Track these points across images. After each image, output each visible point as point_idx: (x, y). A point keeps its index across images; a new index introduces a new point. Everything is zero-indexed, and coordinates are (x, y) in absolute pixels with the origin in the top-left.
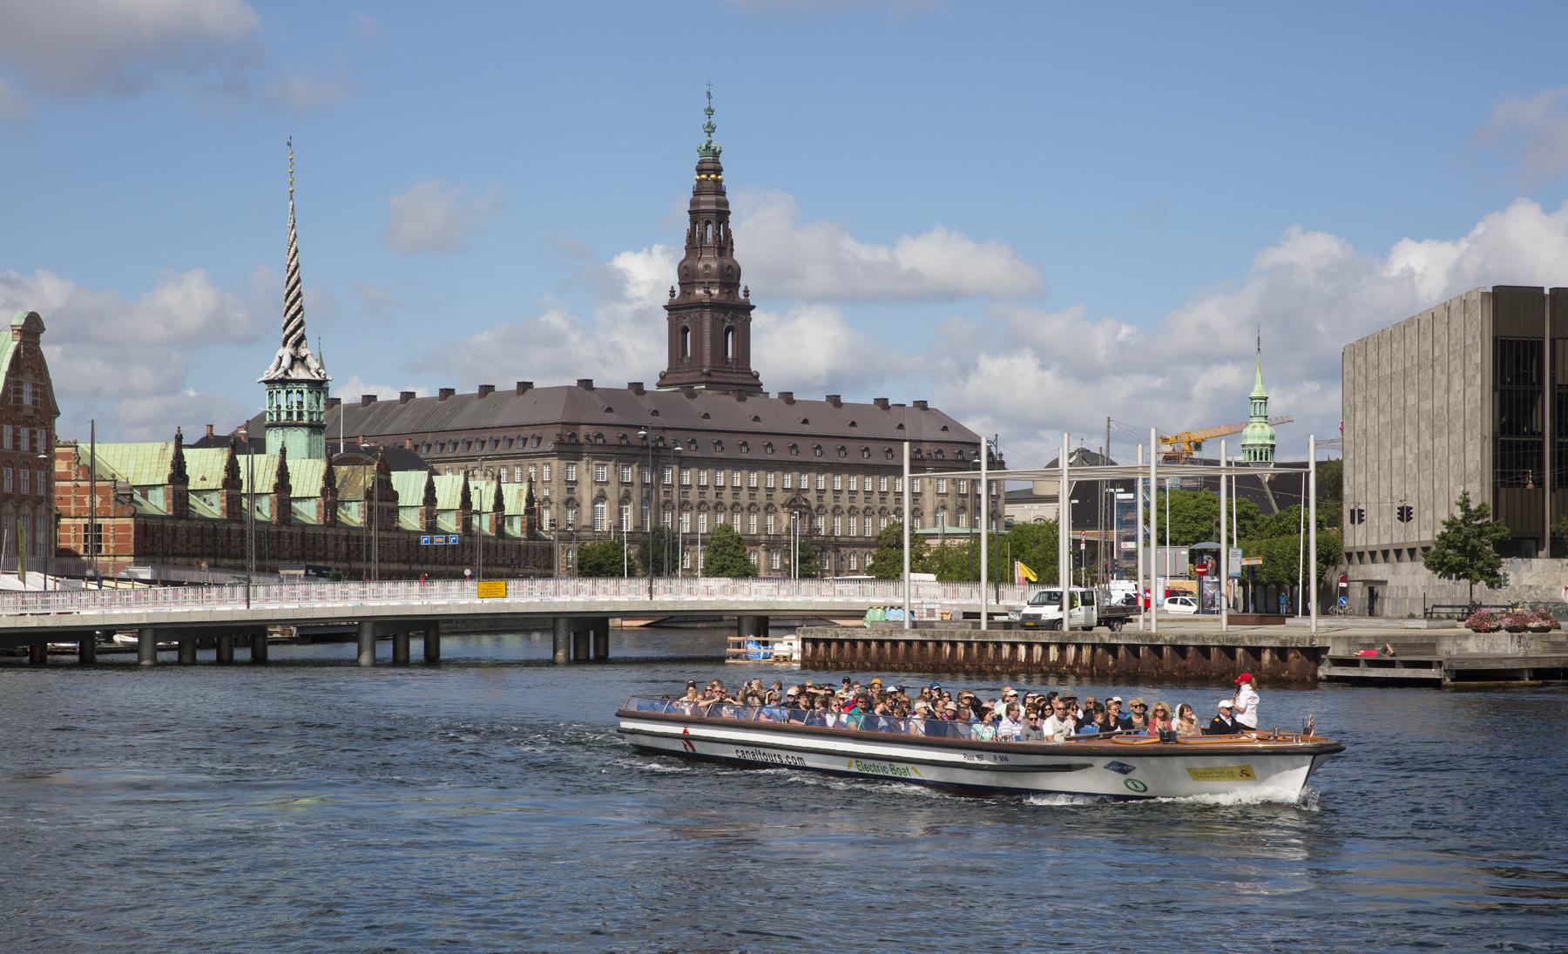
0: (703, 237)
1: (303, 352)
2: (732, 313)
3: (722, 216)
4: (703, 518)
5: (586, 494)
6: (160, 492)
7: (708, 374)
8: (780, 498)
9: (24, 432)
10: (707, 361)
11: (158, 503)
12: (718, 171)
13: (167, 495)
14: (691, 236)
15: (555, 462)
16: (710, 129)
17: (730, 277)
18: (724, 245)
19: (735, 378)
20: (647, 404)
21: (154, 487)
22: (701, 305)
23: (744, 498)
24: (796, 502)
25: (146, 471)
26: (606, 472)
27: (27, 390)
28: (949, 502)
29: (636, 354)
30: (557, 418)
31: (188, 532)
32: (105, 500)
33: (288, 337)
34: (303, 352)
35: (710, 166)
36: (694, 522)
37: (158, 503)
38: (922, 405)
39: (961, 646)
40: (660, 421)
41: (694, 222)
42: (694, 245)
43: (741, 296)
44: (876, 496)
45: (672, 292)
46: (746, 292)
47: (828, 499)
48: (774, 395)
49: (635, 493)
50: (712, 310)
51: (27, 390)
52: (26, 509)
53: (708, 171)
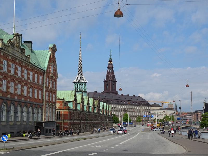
0: (109, 71)
7: (111, 91)
8: (123, 109)
10: (111, 89)
12: (112, 62)
13: (73, 104)
18: (113, 72)
19: (114, 92)
21: (70, 102)
23: (118, 110)
25: (67, 98)
32: (61, 105)
33: (79, 73)
35: (110, 61)
40: (107, 98)
43: (115, 80)
45: (105, 79)
46: (116, 79)
47: (129, 109)
53: (111, 62)
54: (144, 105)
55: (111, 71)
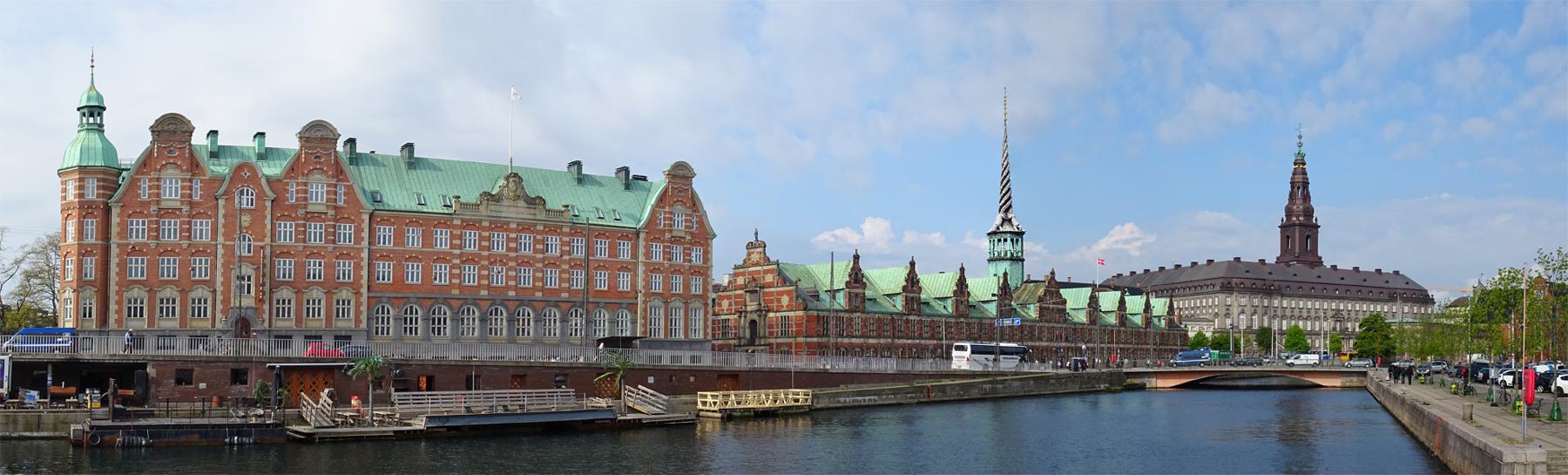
3: (1306, 184)
5: (1235, 310)
8: (1330, 314)
16: (1300, 145)
17: (1309, 212)
18: (1307, 197)
19: (1310, 259)
24: (1337, 316)
26: (1243, 301)
29: (1265, 246)
31: (865, 321)
38: (1397, 273)
40: (1273, 277)
42: (1292, 196)
47: (1353, 315)
49: (1259, 310)
50: (1300, 228)
54: (1406, 300)
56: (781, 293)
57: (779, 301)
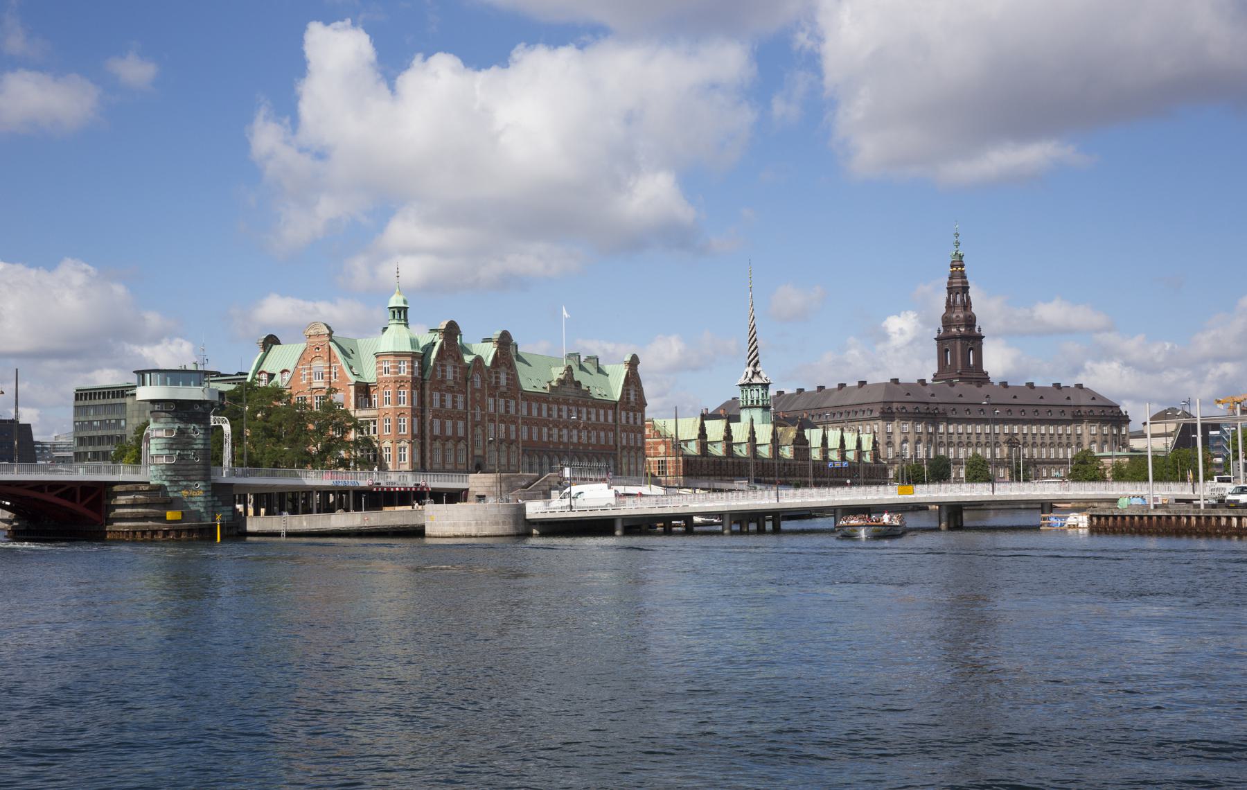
0: (955, 301)
1: (758, 369)
2: (973, 341)
3: (965, 289)
4: (962, 451)
5: (897, 439)
6: (694, 443)
8: (1002, 439)
9: (631, 414)
10: (959, 367)
11: (693, 449)
12: (962, 266)
14: (948, 301)
15: (880, 423)
16: (958, 244)
17: (970, 321)
18: (967, 305)
19: (975, 375)
20: (928, 391)
22: (955, 337)
24: (1012, 442)
26: (907, 427)
27: (632, 393)
28: (1098, 438)
30: (881, 399)
34: (758, 369)
36: (957, 453)
37: (693, 449)
39: (1193, 519)
40: (937, 399)
41: (950, 294)
42: (950, 306)
44: (1056, 437)
47: (1029, 438)
48: (997, 384)
49: (924, 438)
51: (632, 393)
52: (633, 453)
53: (957, 266)
54: (1093, 420)
55: (962, 300)
56: (659, 443)
57: (656, 449)
